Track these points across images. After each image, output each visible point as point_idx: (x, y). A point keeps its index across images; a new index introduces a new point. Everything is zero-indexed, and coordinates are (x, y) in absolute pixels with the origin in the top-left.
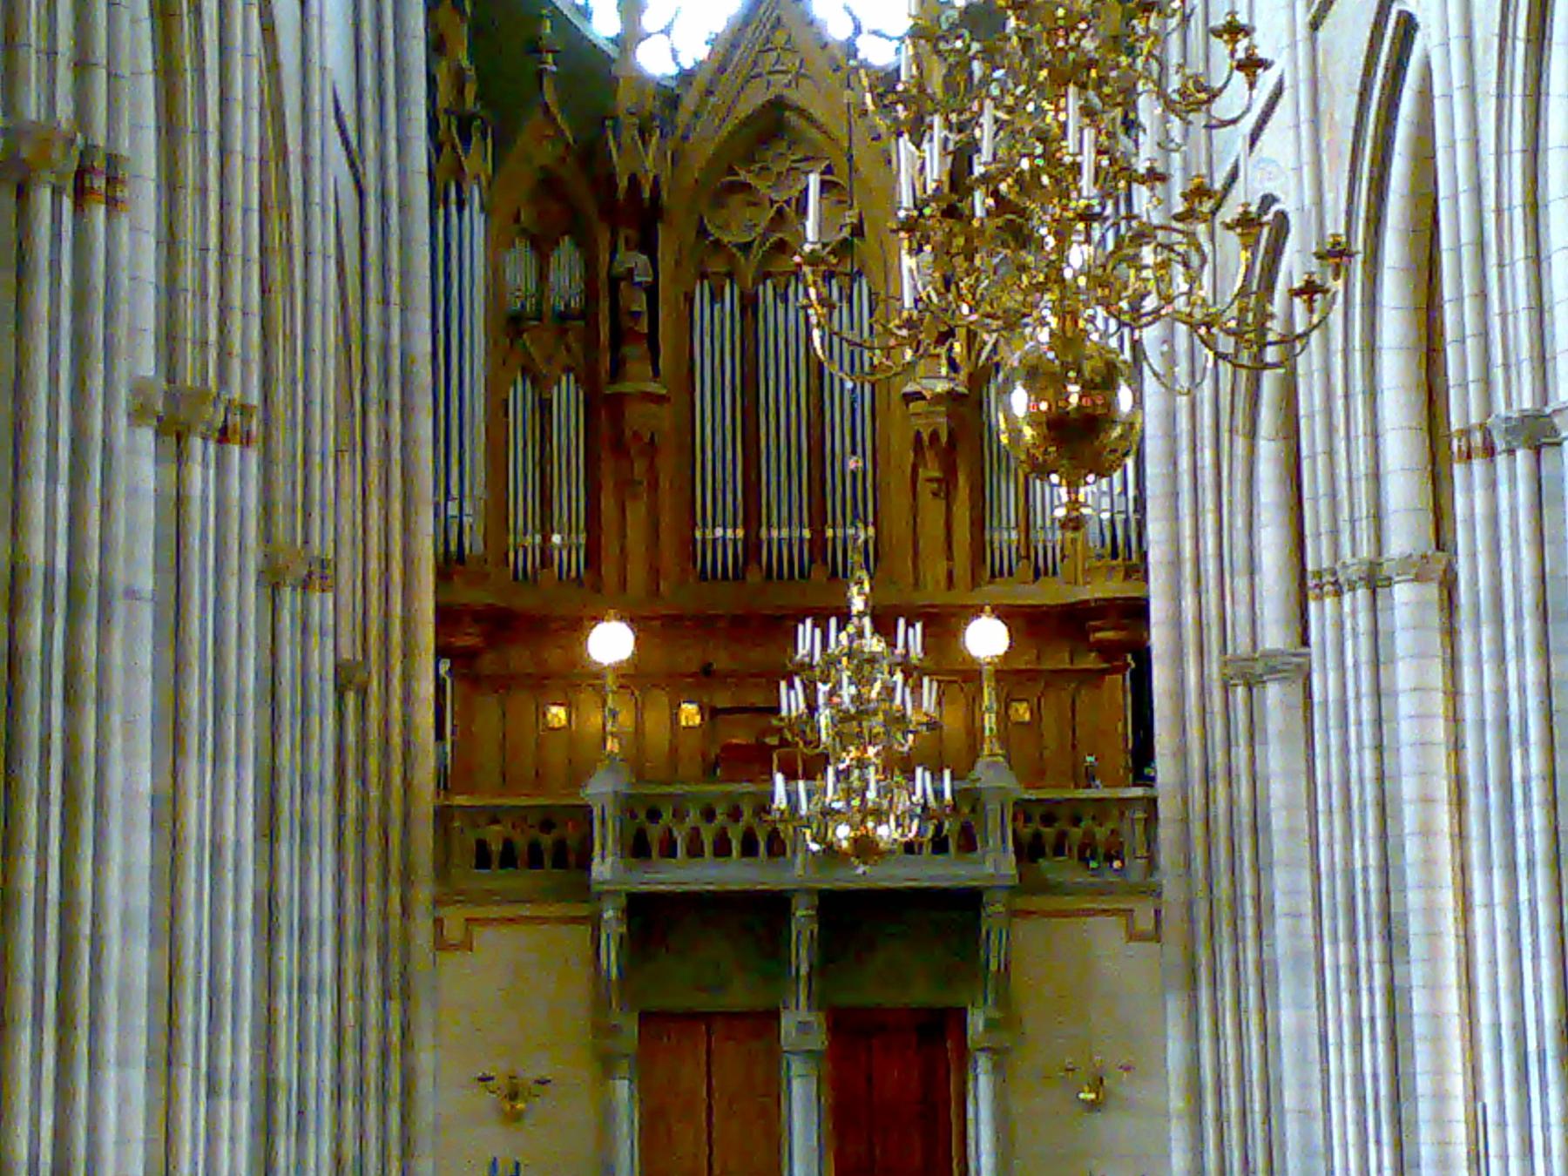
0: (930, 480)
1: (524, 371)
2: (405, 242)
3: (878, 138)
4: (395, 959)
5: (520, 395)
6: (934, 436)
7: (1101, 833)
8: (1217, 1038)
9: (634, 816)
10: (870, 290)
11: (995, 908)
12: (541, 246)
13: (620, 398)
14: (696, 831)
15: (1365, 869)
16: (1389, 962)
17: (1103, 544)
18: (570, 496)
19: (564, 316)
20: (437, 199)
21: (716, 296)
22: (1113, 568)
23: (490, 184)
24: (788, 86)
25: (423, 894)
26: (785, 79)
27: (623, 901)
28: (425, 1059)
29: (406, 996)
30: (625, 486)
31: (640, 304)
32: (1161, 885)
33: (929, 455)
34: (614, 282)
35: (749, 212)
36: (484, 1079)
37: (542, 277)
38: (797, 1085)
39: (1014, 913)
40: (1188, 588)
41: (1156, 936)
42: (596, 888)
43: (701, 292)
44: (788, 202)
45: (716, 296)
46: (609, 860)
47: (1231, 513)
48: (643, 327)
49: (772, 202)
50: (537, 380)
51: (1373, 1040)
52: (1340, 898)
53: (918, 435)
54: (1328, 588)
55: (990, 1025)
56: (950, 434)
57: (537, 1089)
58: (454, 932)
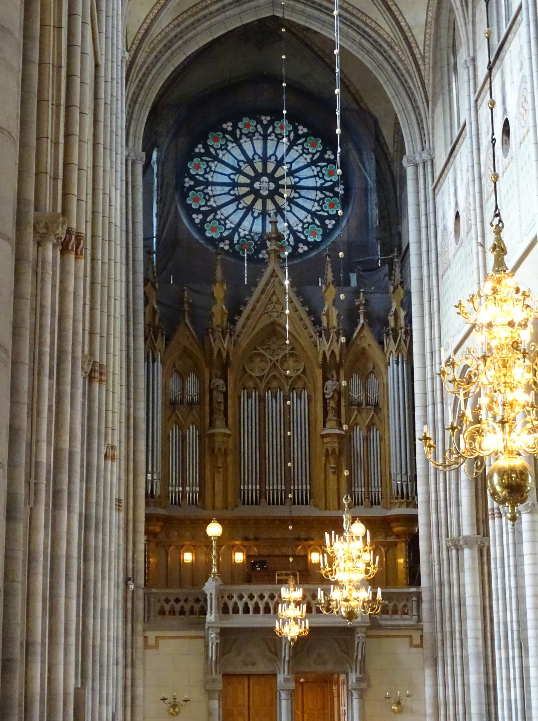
0: (332, 468)
1: (176, 423)
2: (136, 375)
3: (311, 337)
4: (129, 651)
5: (174, 433)
6: (333, 450)
7: (400, 605)
8: (445, 685)
9: (223, 597)
11: (360, 634)
12: (183, 378)
13: (213, 435)
14: (246, 604)
15: (512, 622)
16: (521, 657)
17: (398, 494)
18: (193, 473)
19: (191, 404)
20: (147, 359)
21: (249, 396)
22: (403, 503)
23: (165, 352)
24: (278, 317)
25: (140, 627)
26: (276, 314)
27: (219, 631)
28: (140, 691)
29: (133, 666)
30: (215, 468)
31: (221, 399)
32: (422, 625)
34: (211, 391)
35: (262, 365)
36: (164, 699)
37: (183, 388)
38: (284, 703)
39: (368, 637)
40: (433, 511)
41: (421, 646)
43: (244, 394)
44: (277, 361)
45: (249, 396)
46: (213, 614)
47: (450, 484)
48: (222, 408)
49: (271, 361)
50: (182, 428)
51: (515, 687)
52: (502, 633)
53: (327, 450)
54: (496, 515)
55: (359, 680)
57: (184, 703)
58: (151, 641)
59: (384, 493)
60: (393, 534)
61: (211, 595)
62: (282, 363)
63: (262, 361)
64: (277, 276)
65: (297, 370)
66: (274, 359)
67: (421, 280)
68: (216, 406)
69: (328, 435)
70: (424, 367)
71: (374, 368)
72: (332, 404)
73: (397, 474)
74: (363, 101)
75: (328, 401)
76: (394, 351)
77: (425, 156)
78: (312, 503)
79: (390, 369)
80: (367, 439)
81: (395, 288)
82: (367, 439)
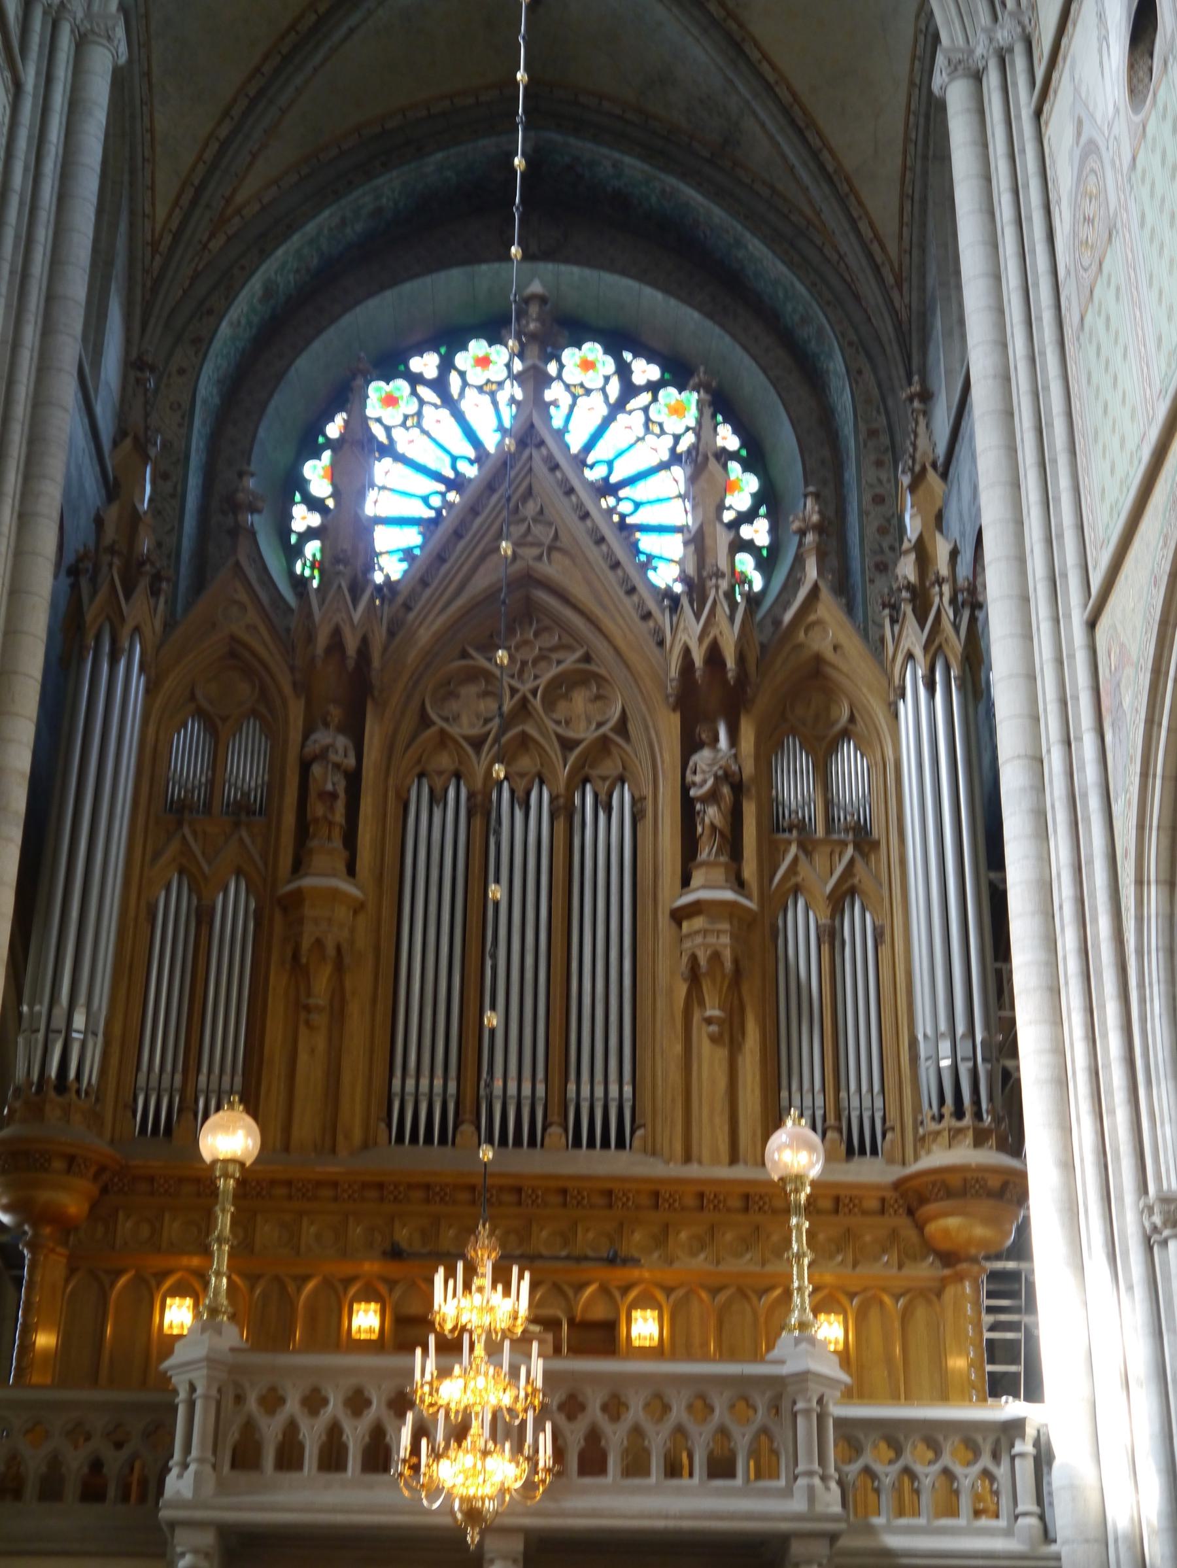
0: (709, 1021)
6: (716, 957)
9: (239, 1399)
10: (633, 797)
13: (298, 897)
14: (335, 1430)
22: (959, 1131)
23: (159, 648)
24: (539, 558)
26: (535, 551)
27: (207, 1539)
30: (300, 1008)
31: (335, 783)
33: (706, 986)
34: (305, 767)
37: (216, 762)
42: (165, 1514)
44: (534, 692)
45: (437, 798)
47: (1142, 1000)
48: (339, 816)
49: (514, 691)
50: (196, 882)
53: (694, 958)
56: (736, 961)
59: (893, 1115)
60: (928, 1248)
61: (192, 1388)
62: (550, 704)
63: (486, 694)
64: (542, 443)
65: (600, 725)
66: (525, 688)
67: (1005, 378)
68: (317, 809)
69: (696, 909)
70: (1027, 635)
71: (852, 719)
72: (712, 814)
73: (938, 1036)
74: (812, 123)
75: (698, 807)
76: (918, 653)
77: (1005, 34)
78: (636, 1143)
79: (906, 710)
80: (831, 936)
81: (918, 480)
82: (831, 936)
